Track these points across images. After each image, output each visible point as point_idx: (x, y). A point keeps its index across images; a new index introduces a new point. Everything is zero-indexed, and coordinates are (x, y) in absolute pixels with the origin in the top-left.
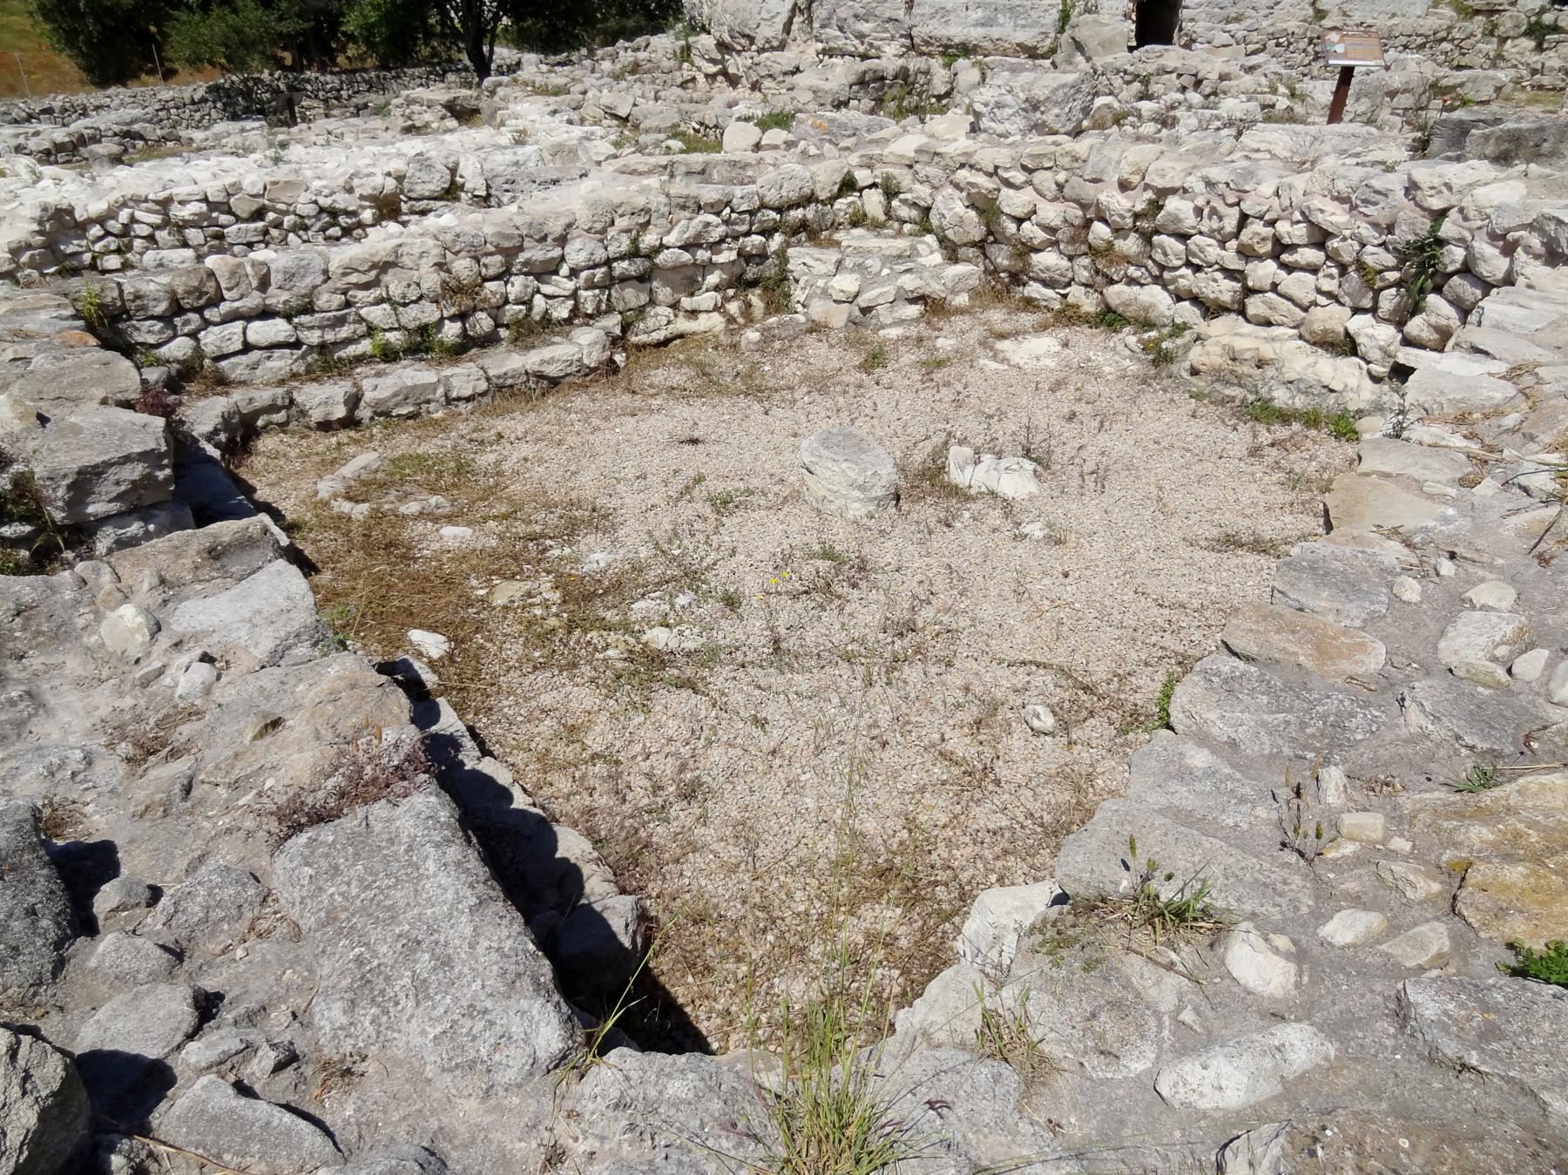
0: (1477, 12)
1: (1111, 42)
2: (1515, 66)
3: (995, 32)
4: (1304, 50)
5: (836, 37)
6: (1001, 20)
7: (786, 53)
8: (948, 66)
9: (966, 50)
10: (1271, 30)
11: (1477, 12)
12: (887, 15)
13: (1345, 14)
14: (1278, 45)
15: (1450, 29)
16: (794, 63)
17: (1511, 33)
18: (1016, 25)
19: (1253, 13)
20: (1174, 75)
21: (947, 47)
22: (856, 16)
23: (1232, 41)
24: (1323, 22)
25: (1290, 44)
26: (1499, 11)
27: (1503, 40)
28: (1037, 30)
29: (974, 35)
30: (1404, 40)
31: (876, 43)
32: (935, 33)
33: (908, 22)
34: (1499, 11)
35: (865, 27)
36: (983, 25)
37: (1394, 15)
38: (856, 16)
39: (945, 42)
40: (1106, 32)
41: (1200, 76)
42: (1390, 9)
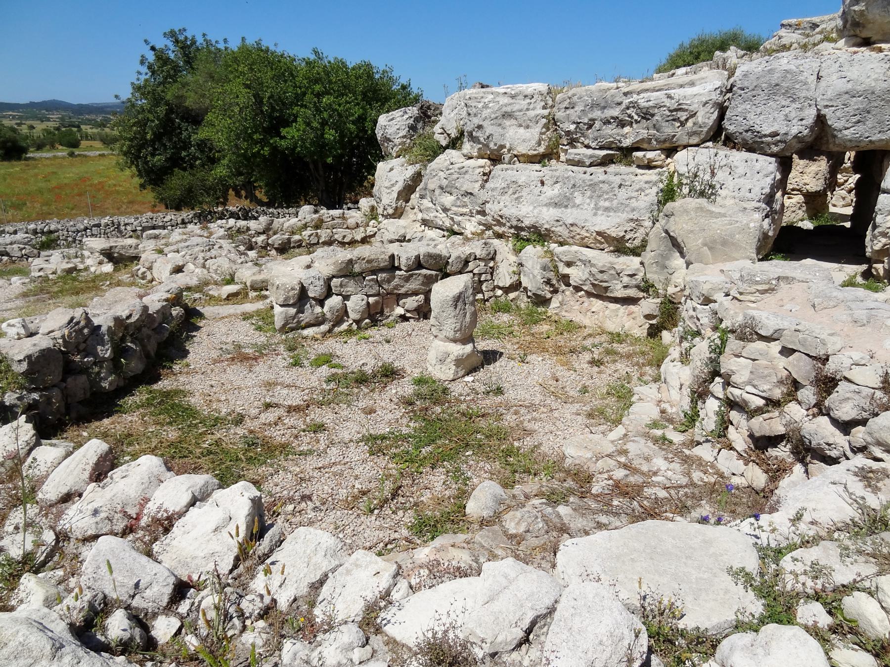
1: (725, 243)
3: (570, 215)
5: (428, 209)
6: (578, 201)
7: (401, 222)
8: (517, 251)
9: (540, 235)
12: (465, 188)
16: (402, 232)
18: (597, 208)
20: (775, 347)
21: (519, 229)
22: (441, 188)
28: (625, 216)
29: (546, 217)
31: (457, 218)
32: (506, 212)
33: (483, 196)
35: (448, 200)
36: (556, 205)
38: (441, 188)
39: (515, 223)
40: (718, 227)
41: (831, 367)
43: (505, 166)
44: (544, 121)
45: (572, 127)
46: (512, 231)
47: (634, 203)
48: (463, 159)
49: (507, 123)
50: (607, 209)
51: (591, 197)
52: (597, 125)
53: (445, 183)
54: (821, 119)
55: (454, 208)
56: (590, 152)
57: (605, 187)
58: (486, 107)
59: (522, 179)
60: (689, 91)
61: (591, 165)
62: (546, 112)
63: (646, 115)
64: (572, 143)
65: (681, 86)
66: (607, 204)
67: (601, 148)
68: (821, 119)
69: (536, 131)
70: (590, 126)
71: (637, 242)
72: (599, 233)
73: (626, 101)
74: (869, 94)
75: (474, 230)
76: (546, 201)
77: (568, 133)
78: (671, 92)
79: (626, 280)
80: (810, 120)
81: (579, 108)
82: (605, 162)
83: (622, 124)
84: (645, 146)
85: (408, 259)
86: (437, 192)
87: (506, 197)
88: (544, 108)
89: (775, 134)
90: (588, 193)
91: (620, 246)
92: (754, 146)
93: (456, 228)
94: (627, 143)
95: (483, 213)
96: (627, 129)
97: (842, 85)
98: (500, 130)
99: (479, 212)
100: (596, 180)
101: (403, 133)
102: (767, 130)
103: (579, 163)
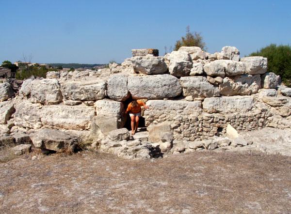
3: (69, 121)
5: (19, 121)
6: (70, 116)
22: (24, 113)
28: (84, 120)
35: (27, 117)
39: (51, 124)
43: (46, 106)
44: (58, 92)
45: (66, 94)
46: (51, 126)
47: (86, 116)
48: (31, 103)
49: (46, 92)
50: (79, 118)
51: (74, 115)
52: (73, 94)
53: (25, 112)
54: (129, 93)
55: (30, 120)
56: (73, 101)
57: (78, 112)
58: (38, 87)
59: (52, 110)
60: (97, 85)
61: (73, 105)
62: (58, 89)
63: (87, 91)
64: (67, 99)
65: (95, 83)
66: (79, 117)
67: (76, 100)
68: (129, 93)
69: (55, 96)
70: (72, 94)
71: (88, 127)
72: (77, 125)
73: (82, 87)
74: (137, 87)
75: (37, 127)
76: (61, 117)
77: (65, 96)
78: (92, 85)
79: (86, 138)
80: (127, 93)
81: (68, 88)
82: (78, 104)
83: (80, 93)
84: (88, 99)
85: (18, 139)
86: (23, 115)
87: (48, 116)
88: (57, 88)
89: (119, 96)
90: (73, 114)
91: (84, 128)
92: (115, 99)
93: (31, 127)
94: (82, 99)
95: (40, 121)
96: (82, 95)
97: (132, 85)
98: (43, 95)
99: (39, 121)
100: (75, 110)
101: (5, 93)
102: (118, 96)
103: (69, 105)
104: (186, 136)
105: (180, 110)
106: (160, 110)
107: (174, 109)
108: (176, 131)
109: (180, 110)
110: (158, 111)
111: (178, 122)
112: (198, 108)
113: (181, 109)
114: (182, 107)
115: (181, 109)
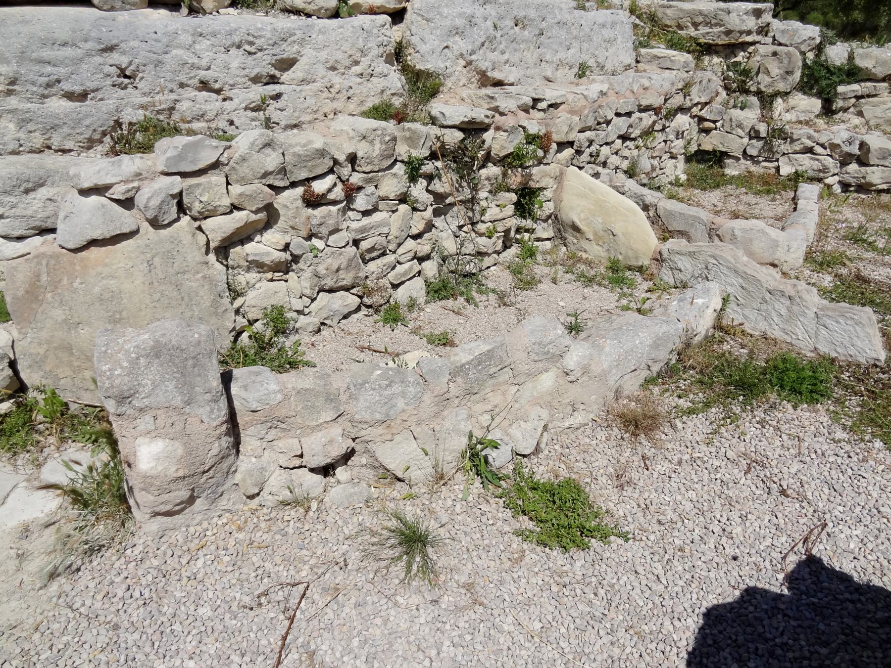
0: (709, 49)
2: (810, 150)
4: (403, 199)
10: (272, 161)
11: (709, 49)
13: (486, 80)
14: (313, 201)
15: (685, 90)
17: (781, 86)
19: (210, 103)
23: (126, 220)
24: (436, 107)
25: (351, 192)
26: (744, 46)
27: (766, 100)
30: (620, 125)
34: (744, 46)
37: (582, 72)
42: (573, 55)
104: (329, 283)
105: (257, 92)
106: (83, 96)
107: (204, 86)
108: (258, 266)
109: (257, 92)
110: (58, 105)
111: (259, 188)
112: (382, 67)
113: (256, 80)
114: (263, 65)
115: (256, 80)
